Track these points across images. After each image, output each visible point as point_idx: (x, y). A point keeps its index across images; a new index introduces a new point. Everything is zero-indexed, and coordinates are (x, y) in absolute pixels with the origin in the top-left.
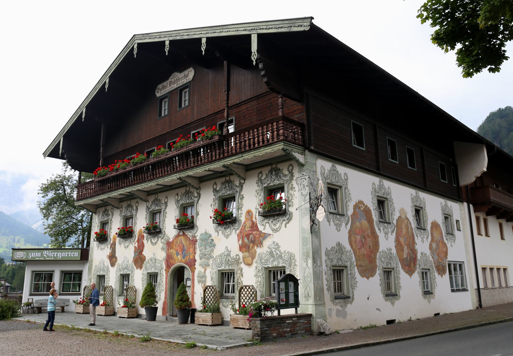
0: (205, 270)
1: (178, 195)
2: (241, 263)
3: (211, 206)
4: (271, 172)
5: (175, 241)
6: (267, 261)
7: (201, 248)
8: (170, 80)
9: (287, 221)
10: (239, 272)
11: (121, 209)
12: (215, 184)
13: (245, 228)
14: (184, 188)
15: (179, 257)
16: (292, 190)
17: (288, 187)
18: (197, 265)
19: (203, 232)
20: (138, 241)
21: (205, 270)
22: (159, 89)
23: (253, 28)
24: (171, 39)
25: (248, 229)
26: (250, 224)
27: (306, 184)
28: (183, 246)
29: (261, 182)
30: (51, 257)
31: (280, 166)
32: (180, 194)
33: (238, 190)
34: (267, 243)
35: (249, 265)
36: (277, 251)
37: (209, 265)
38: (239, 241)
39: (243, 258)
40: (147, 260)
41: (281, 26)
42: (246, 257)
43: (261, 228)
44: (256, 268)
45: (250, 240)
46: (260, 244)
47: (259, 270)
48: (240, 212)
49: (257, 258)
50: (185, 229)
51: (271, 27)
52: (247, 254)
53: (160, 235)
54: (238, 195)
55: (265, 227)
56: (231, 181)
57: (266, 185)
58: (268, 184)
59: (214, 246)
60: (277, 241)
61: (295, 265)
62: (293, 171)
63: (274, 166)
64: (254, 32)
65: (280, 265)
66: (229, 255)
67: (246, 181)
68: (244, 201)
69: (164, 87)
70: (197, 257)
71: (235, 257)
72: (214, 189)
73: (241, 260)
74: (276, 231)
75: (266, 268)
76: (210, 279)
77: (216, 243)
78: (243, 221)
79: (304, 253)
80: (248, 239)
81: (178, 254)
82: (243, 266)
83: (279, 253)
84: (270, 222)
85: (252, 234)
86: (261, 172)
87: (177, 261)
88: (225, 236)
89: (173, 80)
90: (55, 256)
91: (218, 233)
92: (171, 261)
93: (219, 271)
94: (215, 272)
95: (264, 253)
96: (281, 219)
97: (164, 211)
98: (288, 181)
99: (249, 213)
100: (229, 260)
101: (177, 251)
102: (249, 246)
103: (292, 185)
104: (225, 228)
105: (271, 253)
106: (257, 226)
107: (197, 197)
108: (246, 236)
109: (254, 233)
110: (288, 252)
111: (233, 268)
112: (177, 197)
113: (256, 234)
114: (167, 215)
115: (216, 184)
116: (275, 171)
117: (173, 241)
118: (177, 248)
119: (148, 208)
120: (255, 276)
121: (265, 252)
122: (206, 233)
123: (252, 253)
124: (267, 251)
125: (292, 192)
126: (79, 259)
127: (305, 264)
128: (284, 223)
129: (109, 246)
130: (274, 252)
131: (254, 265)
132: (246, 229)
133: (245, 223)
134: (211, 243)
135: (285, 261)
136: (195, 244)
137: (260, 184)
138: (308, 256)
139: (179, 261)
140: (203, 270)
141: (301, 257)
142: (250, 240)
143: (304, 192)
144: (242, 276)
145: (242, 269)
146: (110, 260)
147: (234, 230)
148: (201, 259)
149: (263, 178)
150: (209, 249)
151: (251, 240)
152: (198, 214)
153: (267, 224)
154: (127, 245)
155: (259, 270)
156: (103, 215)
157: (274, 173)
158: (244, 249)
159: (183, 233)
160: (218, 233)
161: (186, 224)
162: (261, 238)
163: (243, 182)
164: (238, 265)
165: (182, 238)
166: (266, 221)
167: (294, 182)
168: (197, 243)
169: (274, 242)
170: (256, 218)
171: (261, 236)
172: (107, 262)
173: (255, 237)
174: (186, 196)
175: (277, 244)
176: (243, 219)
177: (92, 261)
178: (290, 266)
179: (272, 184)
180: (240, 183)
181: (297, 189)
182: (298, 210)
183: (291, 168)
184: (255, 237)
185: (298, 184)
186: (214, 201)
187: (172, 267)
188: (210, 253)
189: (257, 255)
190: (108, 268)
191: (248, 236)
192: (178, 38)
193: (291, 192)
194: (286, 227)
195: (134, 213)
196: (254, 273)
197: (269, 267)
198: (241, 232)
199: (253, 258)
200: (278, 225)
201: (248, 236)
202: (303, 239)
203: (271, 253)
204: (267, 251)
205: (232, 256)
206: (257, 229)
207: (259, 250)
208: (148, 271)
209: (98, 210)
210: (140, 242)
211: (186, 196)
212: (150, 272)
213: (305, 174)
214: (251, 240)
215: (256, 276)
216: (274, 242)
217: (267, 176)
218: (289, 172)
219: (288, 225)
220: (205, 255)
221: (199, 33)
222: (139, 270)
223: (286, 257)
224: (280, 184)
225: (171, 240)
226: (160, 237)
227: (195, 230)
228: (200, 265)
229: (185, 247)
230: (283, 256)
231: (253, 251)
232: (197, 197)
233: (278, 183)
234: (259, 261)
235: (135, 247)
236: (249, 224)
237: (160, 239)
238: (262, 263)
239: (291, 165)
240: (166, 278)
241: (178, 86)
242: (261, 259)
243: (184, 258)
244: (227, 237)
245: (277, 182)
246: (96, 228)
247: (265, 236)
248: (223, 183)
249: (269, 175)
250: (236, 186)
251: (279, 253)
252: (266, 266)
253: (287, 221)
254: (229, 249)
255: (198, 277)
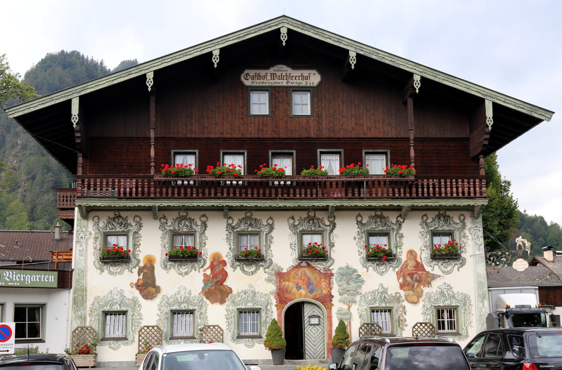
0: (349, 307)
1: (293, 218)
2: (404, 301)
3: (355, 238)
4: (439, 217)
5: (293, 273)
6: (437, 300)
7: (341, 283)
8: (272, 70)
9: (459, 266)
10: (401, 309)
11: (163, 221)
12: (359, 215)
13: (407, 267)
14: (306, 212)
15: (303, 291)
16: (465, 238)
17: (460, 235)
18: (335, 301)
19: (344, 265)
20: (212, 267)
21: (349, 307)
22: (247, 74)
23: (489, 95)
24: (361, 53)
25: (411, 269)
26: (414, 264)
27: (480, 235)
28: (309, 279)
29: (426, 225)
30: (16, 281)
31: (448, 213)
32: (297, 218)
33: (395, 227)
34: (436, 284)
35: (415, 303)
36: (449, 292)
37: (355, 302)
38: (399, 279)
39: (406, 296)
40: (235, 292)
41: (522, 106)
42: (409, 295)
43: (428, 269)
44: (424, 306)
45: (414, 279)
46: (429, 284)
47: (427, 309)
48: (399, 250)
49: (424, 297)
50: (311, 260)
51: (510, 102)
52: (411, 293)
53: (261, 263)
54: (395, 232)
55: (434, 268)
56: (384, 217)
57: (433, 228)
58: (435, 228)
59: (362, 282)
60: (448, 282)
61: (470, 305)
62: (466, 221)
63: (442, 212)
64: (489, 98)
65: (454, 304)
66: (385, 291)
67: (406, 221)
68: (404, 240)
69: (259, 76)
70: (335, 292)
71: (394, 295)
72: (358, 222)
73: (403, 298)
74: (448, 273)
75: (435, 307)
76: (358, 316)
77: (364, 279)
78: (403, 261)
79: (479, 295)
80: (412, 278)
81: (299, 288)
82: (405, 303)
83: (451, 294)
84: (440, 264)
85: (416, 273)
86: (426, 215)
87: (298, 296)
88: (378, 273)
89: (279, 74)
90: (22, 279)
91: (367, 269)
92: (287, 295)
93: (370, 308)
94: (366, 309)
95: (433, 292)
96: (453, 263)
97: (267, 234)
98: (459, 229)
99: (411, 252)
100: (385, 297)
101: (297, 284)
102: (413, 286)
103: (465, 234)
104: (377, 265)
105: (442, 293)
106: (422, 266)
107: (330, 225)
108: (409, 274)
109: (419, 273)
110: (462, 293)
111: (391, 306)
112: (291, 221)
113: (422, 274)
114: (273, 240)
115: (361, 216)
116: (444, 217)
117: (288, 273)
118: (297, 281)
119: (230, 227)
120: (422, 314)
121: (435, 292)
122: (348, 268)
123: (418, 292)
124: (437, 291)
125: (465, 240)
126: (56, 286)
127: (481, 305)
128: (457, 267)
129: (136, 270)
130: (445, 293)
131: (421, 303)
132: (408, 268)
133: (406, 262)
134: (356, 278)
135: (457, 301)
136: (330, 279)
137: (424, 226)
138: (484, 298)
139: (300, 295)
140: (345, 307)
141: (476, 298)
142: (414, 279)
143: (478, 242)
144: (405, 313)
145: (404, 307)
146: (141, 292)
147: (391, 268)
148: (341, 294)
149: (428, 221)
150: (353, 285)
151: (414, 278)
152: (332, 245)
153: (436, 266)
154: (184, 271)
155: (427, 309)
156: (109, 223)
157: (442, 218)
158: (406, 288)
159: (308, 264)
160: (367, 269)
161: (314, 256)
162: (429, 279)
163: (402, 220)
164: (399, 302)
165: (307, 271)
166: (434, 263)
167: (466, 231)
168: (334, 277)
169: (445, 284)
170: (421, 259)
171: (428, 277)
172: (132, 293)
173: (420, 277)
174: (309, 222)
175: (449, 286)
176: (403, 257)
177: (84, 290)
178: (465, 305)
179: (440, 229)
180: (398, 221)
181: (470, 237)
182: (472, 257)
183: (462, 218)
184: (420, 277)
185: (471, 234)
186: (359, 234)
187: (290, 304)
188: (356, 289)
189: (424, 294)
190: (135, 302)
191: (411, 275)
192: (374, 57)
193: (463, 239)
194: (458, 270)
195: (198, 229)
196: (422, 311)
197: (439, 306)
198: (401, 271)
199: (419, 296)
200: (449, 268)
201: (411, 275)
202: (478, 282)
203: (442, 293)
204: (437, 291)
205: (389, 293)
206: (424, 270)
207: (426, 290)
208: (239, 307)
209: (92, 214)
210: (217, 270)
211: (309, 222)
212: (244, 307)
213: (478, 225)
214: (414, 278)
215: (424, 313)
216: (445, 284)
217: (434, 220)
218: (461, 221)
219: (460, 269)
220: (348, 291)
221: (411, 67)
222: (217, 306)
223: (460, 298)
224: (450, 230)
225: (285, 271)
226: (263, 266)
227: (329, 263)
228: (341, 301)
229: (313, 280)
230: (456, 296)
231: (418, 289)
232: (330, 225)
233: (449, 228)
234: (427, 300)
235: (205, 275)
236: (411, 264)
237: (261, 268)
238: (430, 301)
239: (463, 215)
240: (279, 315)
241: (290, 84)
242: (429, 298)
243: (311, 292)
244: (382, 274)
245: (446, 228)
246: (91, 241)
247: (434, 277)
248: (371, 217)
249: (437, 219)
250: (392, 223)
251: (451, 294)
252: (436, 305)
253: (459, 266)
254: (385, 286)
255: (337, 314)
